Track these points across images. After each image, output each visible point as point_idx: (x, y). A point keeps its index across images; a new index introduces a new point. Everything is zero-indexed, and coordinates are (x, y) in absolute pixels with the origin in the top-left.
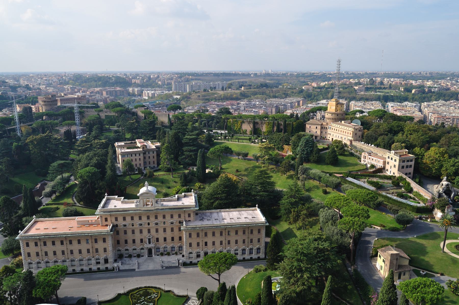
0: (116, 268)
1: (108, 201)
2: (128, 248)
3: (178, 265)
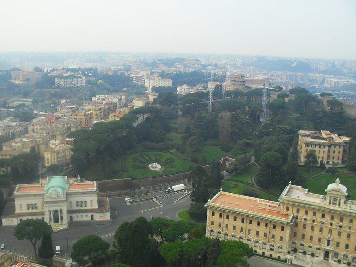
1: (291, 190)
2: (304, 244)
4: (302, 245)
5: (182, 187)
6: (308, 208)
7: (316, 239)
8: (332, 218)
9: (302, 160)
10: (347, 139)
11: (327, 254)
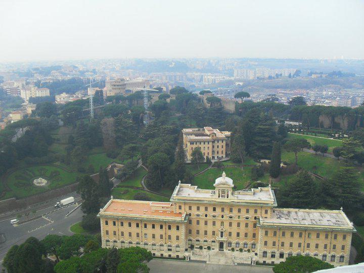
1: (181, 189)
2: (200, 239)
3: (250, 263)
4: (199, 241)
5: (72, 199)
6: (199, 204)
7: (210, 233)
8: (223, 210)
9: (189, 158)
10: (228, 133)
11: (221, 245)
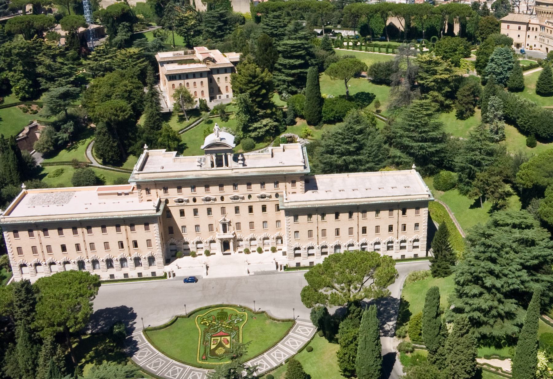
0: (169, 273)
